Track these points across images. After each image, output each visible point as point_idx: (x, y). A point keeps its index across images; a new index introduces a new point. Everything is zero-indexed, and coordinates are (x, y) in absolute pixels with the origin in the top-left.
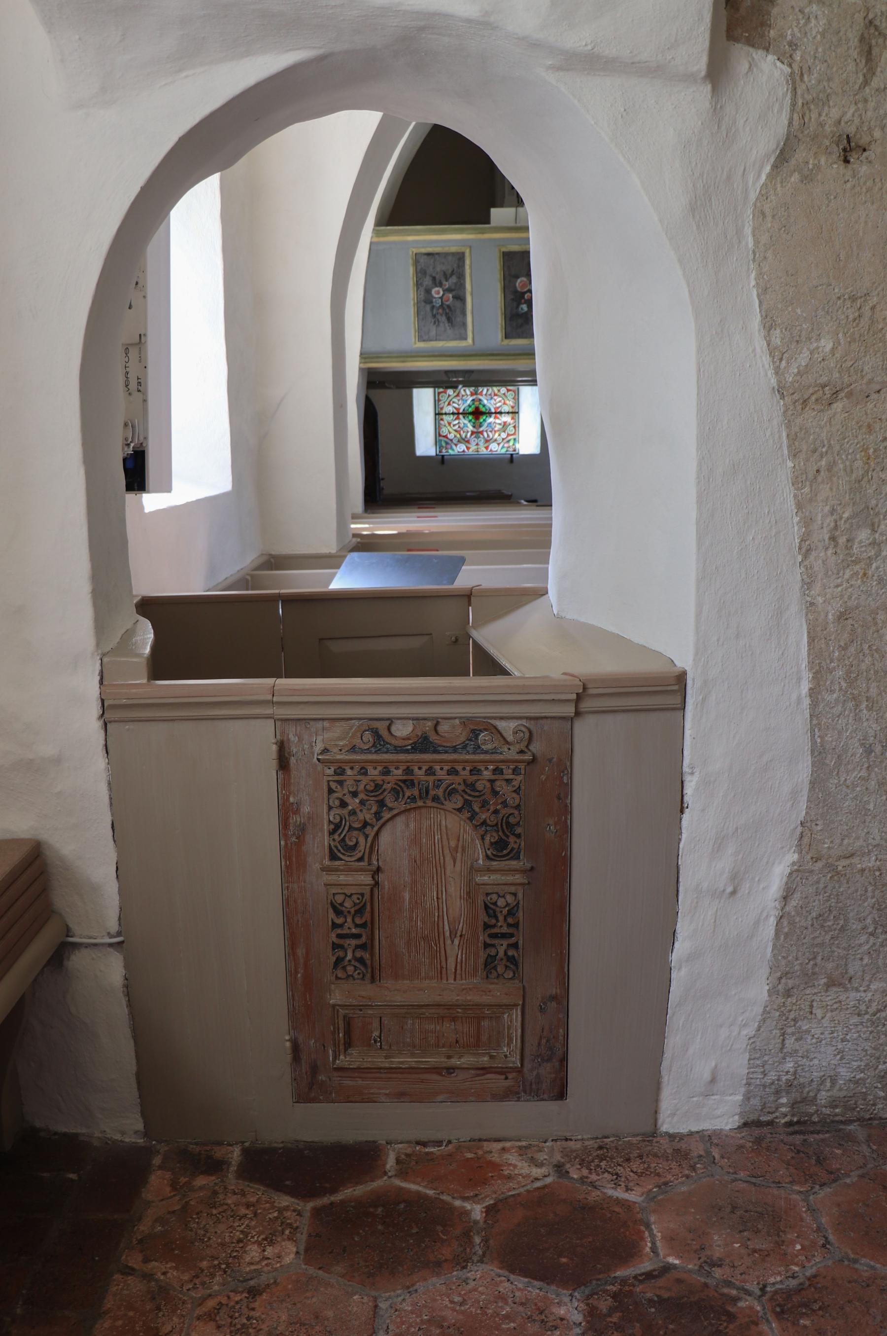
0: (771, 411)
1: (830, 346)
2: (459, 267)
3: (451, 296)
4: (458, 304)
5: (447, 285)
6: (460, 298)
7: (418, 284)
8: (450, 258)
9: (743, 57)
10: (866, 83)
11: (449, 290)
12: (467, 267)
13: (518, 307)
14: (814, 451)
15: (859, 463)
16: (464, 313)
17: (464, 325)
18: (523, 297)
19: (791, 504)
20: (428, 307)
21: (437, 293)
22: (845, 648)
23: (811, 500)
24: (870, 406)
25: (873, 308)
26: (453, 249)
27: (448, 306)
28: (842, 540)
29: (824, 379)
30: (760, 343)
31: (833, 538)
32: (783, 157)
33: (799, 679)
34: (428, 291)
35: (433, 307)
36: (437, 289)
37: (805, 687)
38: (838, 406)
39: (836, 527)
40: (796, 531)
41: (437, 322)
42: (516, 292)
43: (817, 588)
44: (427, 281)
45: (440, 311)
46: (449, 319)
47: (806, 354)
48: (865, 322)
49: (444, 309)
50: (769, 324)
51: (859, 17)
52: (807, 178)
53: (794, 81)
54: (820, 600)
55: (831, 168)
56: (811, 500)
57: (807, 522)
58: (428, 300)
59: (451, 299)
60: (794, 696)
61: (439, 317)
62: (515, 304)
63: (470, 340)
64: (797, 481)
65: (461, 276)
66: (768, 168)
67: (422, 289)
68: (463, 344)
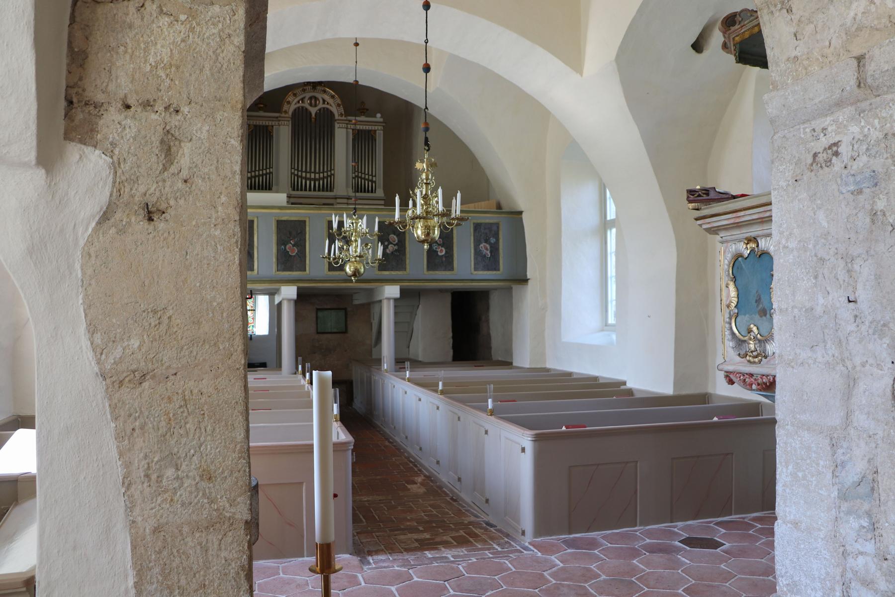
0: (97, 390)
1: (137, 344)
9: (74, 151)
10: (165, 169)
14: (130, 415)
15: (163, 424)
19: (114, 453)
22: (160, 552)
23: (129, 450)
24: (169, 384)
25: (170, 318)
28: (154, 477)
29: (134, 367)
30: (85, 343)
31: (147, 476)
32: (105, 216)
33: (126, 576)
37: (131, 582)
38: (146, 385)
39: (149, 468)
40: (120, 472)
43: (137, 511)
47: (120, 349)
48: (163, 327)
50: (92, 329)
51: (160, 129)
52: (121, 231)
53: (115, 166)
54: (140, 519)
55: (140, 225)
56: (129, 450)
57: (127, 465)
60: (123, 588)
64: (119, 437)
66: (93, 224)
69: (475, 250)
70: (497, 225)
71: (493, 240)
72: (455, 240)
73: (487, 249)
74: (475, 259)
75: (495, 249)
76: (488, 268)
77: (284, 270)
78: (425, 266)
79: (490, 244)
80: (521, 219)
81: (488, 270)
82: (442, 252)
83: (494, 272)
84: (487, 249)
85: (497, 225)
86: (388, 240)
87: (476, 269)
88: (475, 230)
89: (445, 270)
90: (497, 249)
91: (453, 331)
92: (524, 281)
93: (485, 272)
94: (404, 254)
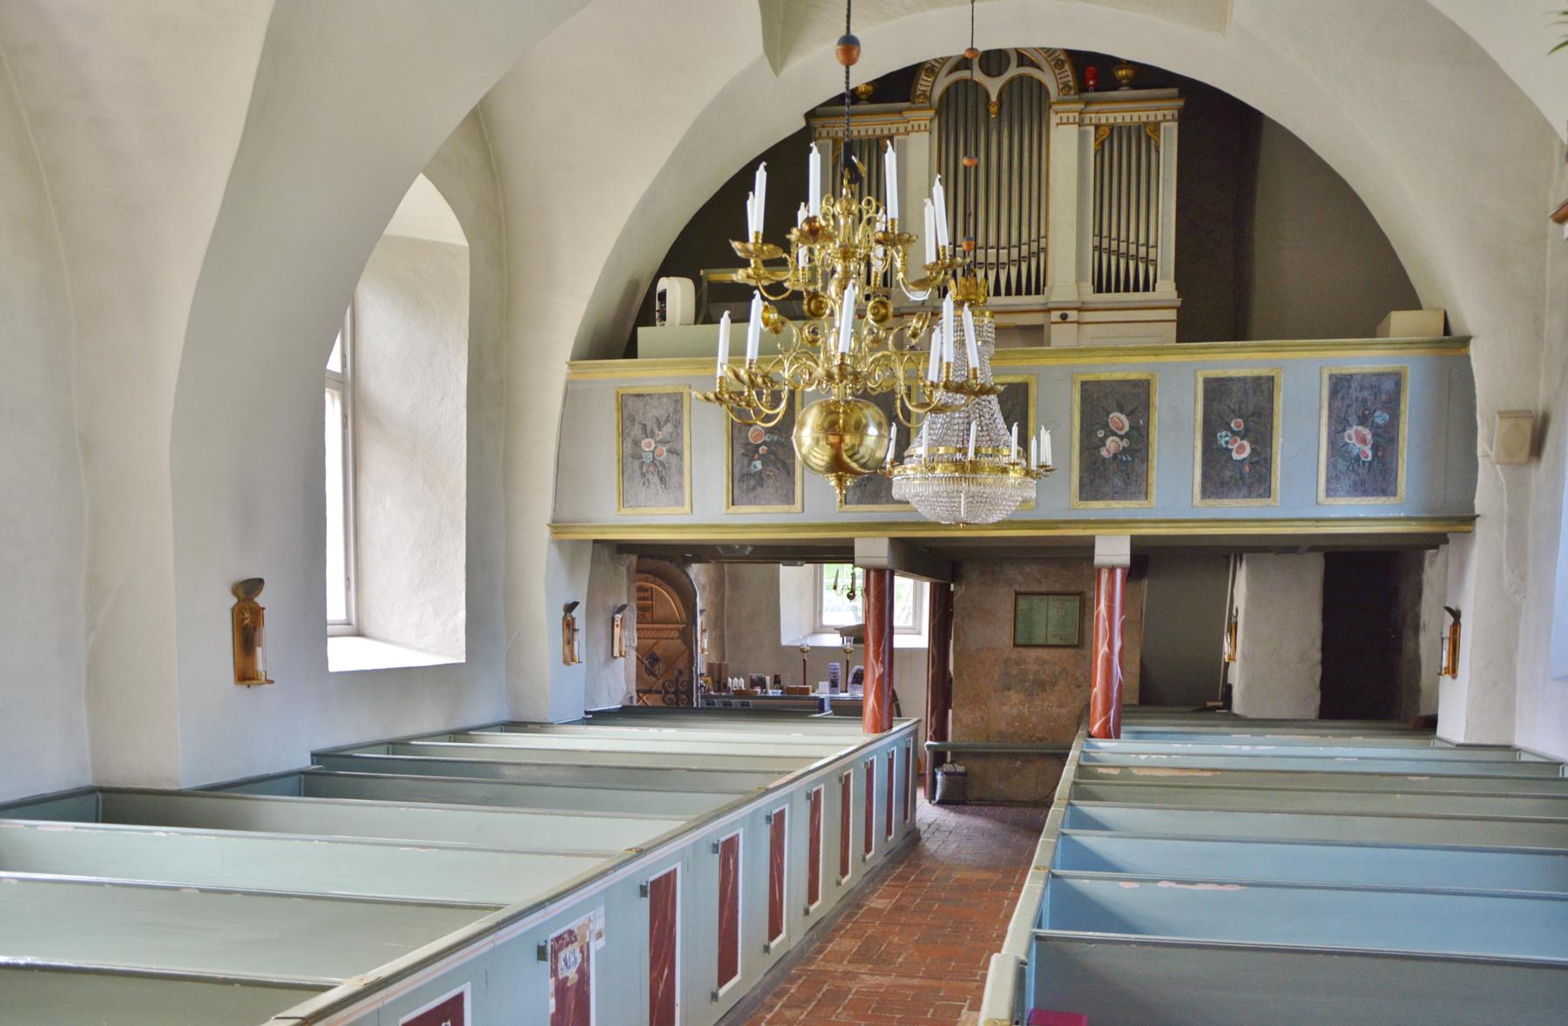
2: (675, 411)
4: (674, 459)
5: (660, 435)
6: (676, 452)
7: (623, 435)
8: (665, 400)
12: (685, 411)
16: (681, 472)
17: (681, 486)
20: (637, 463)
21: (647, 445)
26: (670, 389)
27: (662, 463)
34: (636, 443)
41: (646, 484)
44: (637, 431)
46: (662, 479)
58: (637, 456)
61: (649, 476)
62: (746, 460)
63: (687, 508)
65: (678, 425)
67: (629, 440)
68: (679, 510)
69: (1332, 443)
70: (1397, 378)
71: (1381, 418)
72: (1278, 421)
73: (1364, 441)
74: (1331, 466)
75: (1385, 441)
76: (1362, 488)
77: (860, 502)
80: (1467, 358)
81: (1366, 493)
82: (1242, 451)
83: (1382, 500)
85: (1397, 378)
86: (1106, 426)
87: (1330, 492)
88: (1334, 393)
89: (1249, 496)
91: (1324, 649)
92: (1471, 519)
93: (1356, 501)
94: (1145, 459)
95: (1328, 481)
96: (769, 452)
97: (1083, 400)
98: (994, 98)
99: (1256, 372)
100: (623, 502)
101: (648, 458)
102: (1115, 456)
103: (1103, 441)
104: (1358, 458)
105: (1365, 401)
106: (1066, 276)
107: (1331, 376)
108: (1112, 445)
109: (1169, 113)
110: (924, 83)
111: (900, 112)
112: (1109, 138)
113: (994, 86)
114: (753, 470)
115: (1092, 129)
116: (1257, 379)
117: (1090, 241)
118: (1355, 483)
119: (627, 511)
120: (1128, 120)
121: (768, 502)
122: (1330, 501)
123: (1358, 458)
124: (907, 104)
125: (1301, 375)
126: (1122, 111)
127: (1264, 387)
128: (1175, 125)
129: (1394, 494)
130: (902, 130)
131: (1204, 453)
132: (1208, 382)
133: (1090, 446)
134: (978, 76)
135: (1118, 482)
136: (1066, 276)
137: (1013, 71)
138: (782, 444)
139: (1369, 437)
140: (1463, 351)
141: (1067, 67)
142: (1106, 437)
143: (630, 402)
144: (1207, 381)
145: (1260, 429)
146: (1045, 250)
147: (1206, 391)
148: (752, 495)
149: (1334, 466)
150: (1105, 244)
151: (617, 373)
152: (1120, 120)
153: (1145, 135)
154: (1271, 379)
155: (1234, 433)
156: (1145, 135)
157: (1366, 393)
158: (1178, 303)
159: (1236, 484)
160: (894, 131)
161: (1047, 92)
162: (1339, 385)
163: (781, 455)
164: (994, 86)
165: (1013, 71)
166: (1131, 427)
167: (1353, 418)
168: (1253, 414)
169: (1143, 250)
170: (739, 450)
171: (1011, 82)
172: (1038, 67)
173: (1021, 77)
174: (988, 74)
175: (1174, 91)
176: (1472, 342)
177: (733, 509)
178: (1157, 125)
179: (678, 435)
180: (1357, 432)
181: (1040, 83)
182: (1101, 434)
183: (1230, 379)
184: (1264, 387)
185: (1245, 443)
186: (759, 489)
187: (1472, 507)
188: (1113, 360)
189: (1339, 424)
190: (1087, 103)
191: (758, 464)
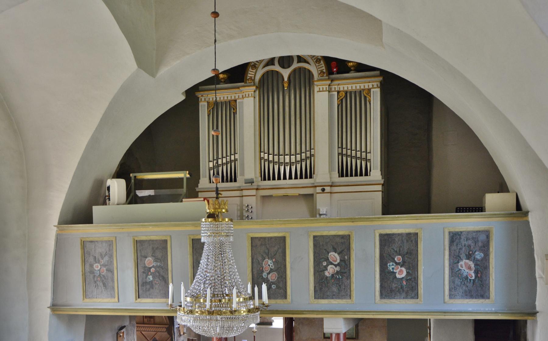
3: (105, 269)
4: (110, 274)
5: (103, 262)
6: (111, 271)
7: (84, 261)
8: (104, 244)
11: (104, 265)
12: (114, 250)
13: (146, 277)
16: (113, 281)
17: (113, 288)
18: (150, 271)
20: (92, 276)
27: (103, 276)
34: (91, 266)
35: (94, 276)
36: (97, 264)
41: (97, 286)
42: (145, 267)
44: (91, 260)
45: (99, 279)
46: (104, 285)
49: (101, 277)
59: (105, 271)
61: (98, 283)
63: (116, 299)
65: (111, 256)
69: (452, 269)
70: (487, 234)
72: (421, 257)
73: (470, 268)
74: (452, 282)
75: (482, 269)
76: (469, 295)
78: (378, 293)
79: (475, 261)
80: (528, 222)
81: (472, 297)
82: (401, 273)
83: (481, 301)
84: (470, 268)
85: (487, 234)
86: (327, 259)
87: (451, 296)
89: (406, 297)
90: (486, 268)
92: (534, 314)
94: (349, 277)
95: (450, 290)
96: (156, 271)
97: (315, 246)
98: (286, 79)
99: (408, 231)
100: (86, 295)
101: (97, 274)
102: (333, 275)
103: (326, 268)
104: (466, 278)
105: (469, 246)
106: (324, 169)
107: (450, 232)
108: (331, 270)
109: (375, 84)
110: (250, 73)
111: (238, 88)
112: (345, 99)
113: (286, 73)
114: (148, 280)
115: (336, 93)
116: (409, 234)
117: (336, 151)
118: (466, 291)
119: (87, 300)
120: (354, 88)
121: (156, 297)
122: (452, 301)
123: (466, 278)
124: (243, 84)
125: (432, 230)
126: (349, 84)
127: (412, 239)
128: (378, 90)
129: (489, 298)
130: (241, 97)
131: (380, 275)
132: (381, 236)
133: (319, 270)
134: (276, 68)
135: (335, 289)
136: (324, 169)
137: (295, 65)
138: (162, 267)
139: (473, 266)
140: (525, 219)
141: (322, 62)
142: (327, 265)
143: (88, 245)
144: (381, 236)
145: (411, 263)
146: (313, 155)
147: (381, 241)
148: (148, 293)
149: (454, 282)
150: (344, 152)
151: (82, 230)
152: (350, 88)
153: (362, 96)
154: (416, 234)
155: (397, 264)
156: (362, 96)
157: (470, 242)
158: (382, 182)
159: (399, 291)
160: (237, 97)
161: (313, 75)
162: (454, 237)
163: (162, 273)
164: (286, 73)
165: (295, 65)
166: (341, 260)
167: (463, 256)
168: (407, 253)
169: (364, 155)
170: (141, 270)
171: (295, 70)
172: (308, 63)
173: (300, 68)
174: (283, 67)
175: (378, 73)
176: (530, 213)
177: (139, 300)
178: (369, 90)
179: (111, 263)
180: (465, 263)
181: (309, 71)
182: (325, 264)
183: (393, 234)
184: (412, 239)
185: (403, 269)
186: (151, 290)
187: (535, 307)
188: (329, 224)
189: (455, 258)
190: (332, 81)
191: (151, 278)
